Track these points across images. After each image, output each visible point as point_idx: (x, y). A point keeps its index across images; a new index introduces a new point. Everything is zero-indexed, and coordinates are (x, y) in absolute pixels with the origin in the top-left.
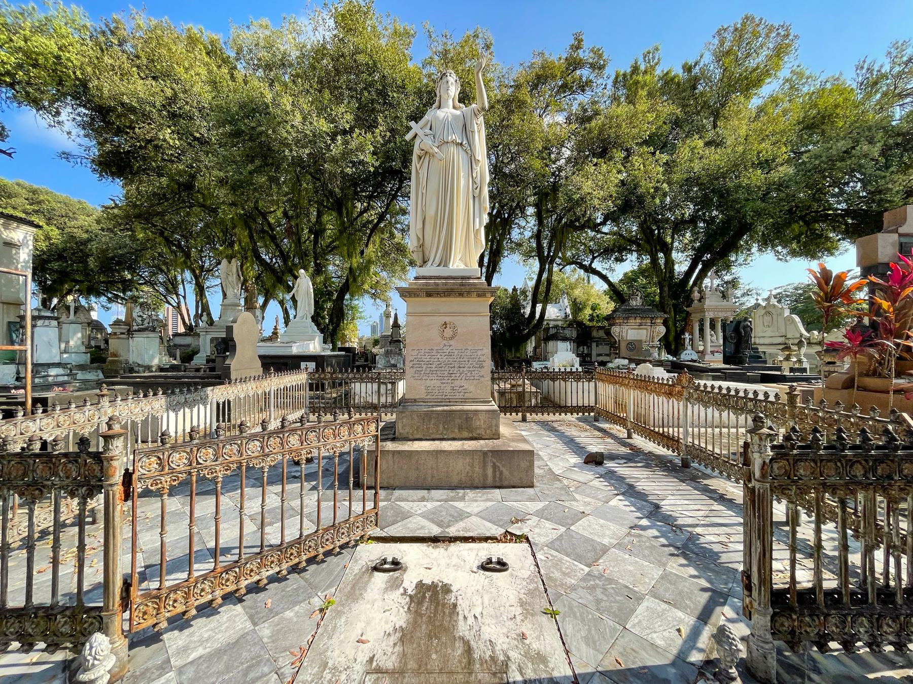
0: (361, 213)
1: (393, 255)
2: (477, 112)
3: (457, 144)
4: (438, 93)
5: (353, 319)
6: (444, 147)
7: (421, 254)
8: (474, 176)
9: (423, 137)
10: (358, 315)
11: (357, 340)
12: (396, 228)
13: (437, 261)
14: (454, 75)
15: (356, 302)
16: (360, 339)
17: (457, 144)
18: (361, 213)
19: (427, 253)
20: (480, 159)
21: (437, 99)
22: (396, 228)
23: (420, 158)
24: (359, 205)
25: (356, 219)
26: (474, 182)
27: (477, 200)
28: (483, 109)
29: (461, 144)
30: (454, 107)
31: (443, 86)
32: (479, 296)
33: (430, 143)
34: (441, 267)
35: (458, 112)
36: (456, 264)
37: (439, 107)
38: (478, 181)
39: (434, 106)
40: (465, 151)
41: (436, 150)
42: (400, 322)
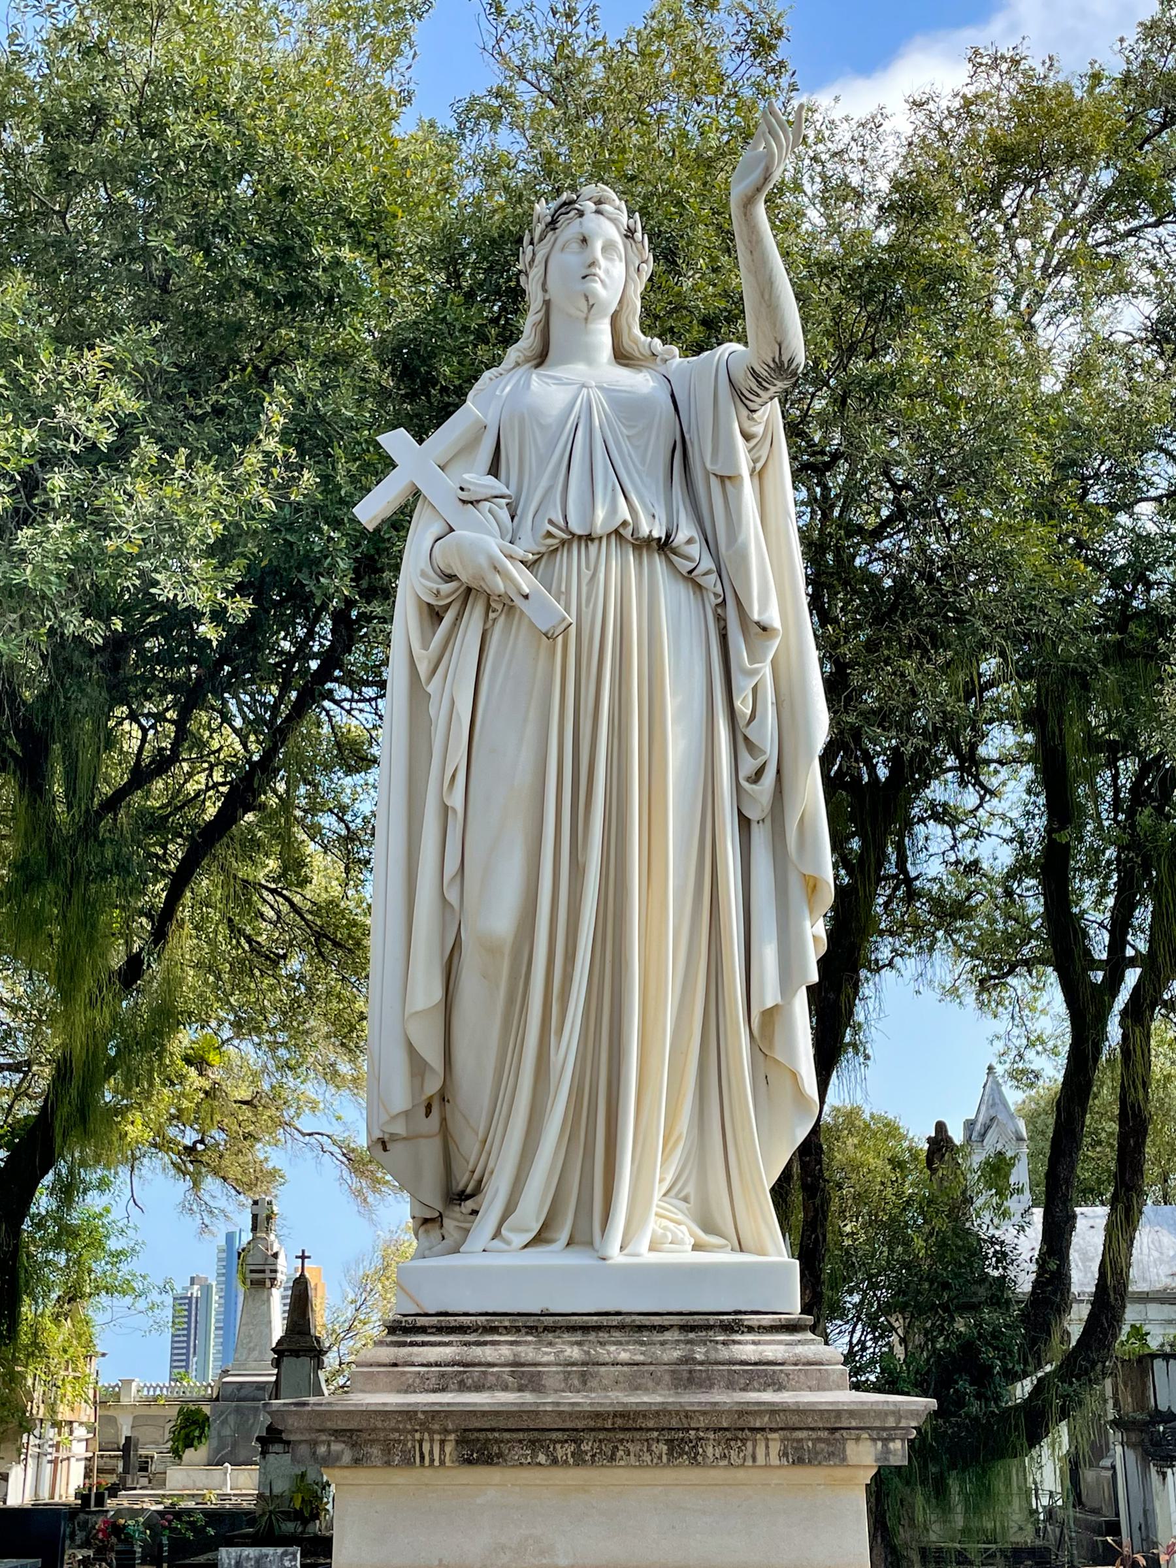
0: (140, 776)
1: (295, 964)
2: (746, 383)
3: (643, 545)
4: (531, 285)
5: (73, 1296)
6: (572, 563)
7: (430, 1151)
8: (744, 707)
9: (452, 512)
10: (99, 1267)
11: (87, 1413)
12: (315, 832)
13: (531, 1212)
14: (616, 206)
15: (94, 1201)
16: (106, 1401)
17: (643, 545)
18: (140, 776)
19: (468, 1146)
20: (774, 618)
21: (529, 324)
22: (315, 832)
23: (435, 614)
24: (131, 737)
25: (113, 803)
26: (741, 741)
27: (760, 837)
28: (781, 368)
29: (664, 546)
30: (621, 356)
31: (565, 260)
32: (798, 1458)
33: (494, 544)
34: (552, 1257)
35: (642, 382)
36: (653, 1226)
37: (541, 358)
38: (766, 733)
39: (513, 353)
40: (690, 578)
41: (525, 580)
42: (322, 1319)
